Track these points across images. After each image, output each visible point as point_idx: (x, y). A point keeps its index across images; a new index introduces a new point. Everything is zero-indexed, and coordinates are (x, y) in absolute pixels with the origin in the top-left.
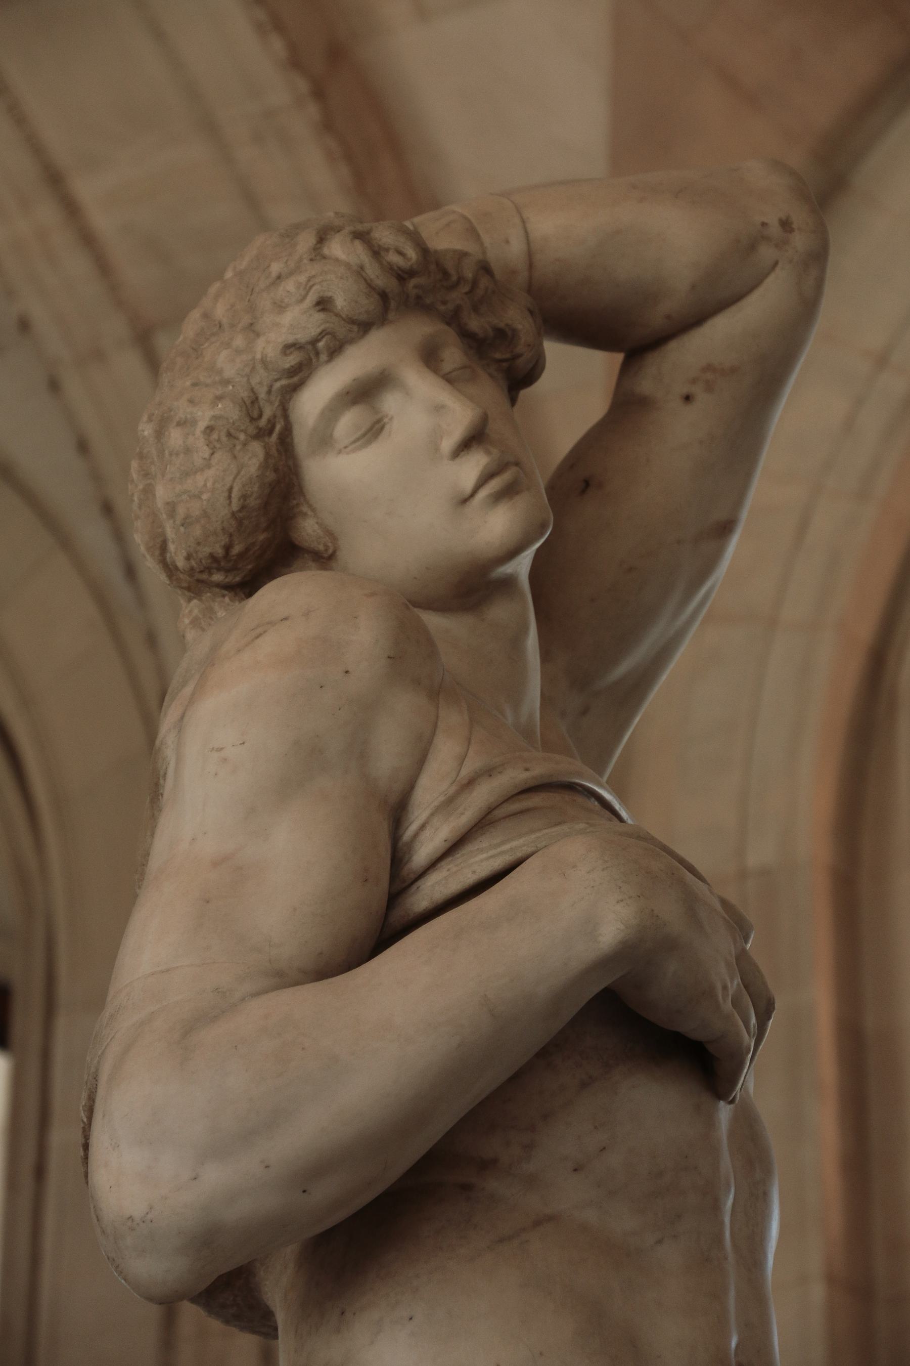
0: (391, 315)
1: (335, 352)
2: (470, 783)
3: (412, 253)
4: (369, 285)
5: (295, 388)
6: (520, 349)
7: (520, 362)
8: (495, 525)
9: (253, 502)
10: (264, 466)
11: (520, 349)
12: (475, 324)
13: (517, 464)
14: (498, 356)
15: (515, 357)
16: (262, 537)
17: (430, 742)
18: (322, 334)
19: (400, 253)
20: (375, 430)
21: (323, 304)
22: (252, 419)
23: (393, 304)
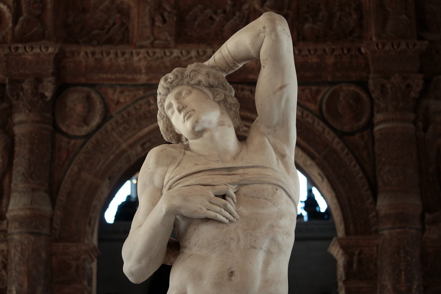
0: (171, 91)
1: (164, 101)
2: (168, 182)
3: (172, 78)
4: (164, 88)
5: (164, 109)
6: (203, 83)
7: (205, 84)
8: (189, 124)
9: (165, 131)
10: (164, 124)
11: (203, 83)
12: (193, 82)
13: (193, 110)
14: (202, 85)
15: (204, 84)
16: (171, 135)
17: (165, 175)
18: (161, 99)
19: (171, 78)
20: (173, 112)
21: (160, 94)
22: (161, 116)
23: (170, 89)
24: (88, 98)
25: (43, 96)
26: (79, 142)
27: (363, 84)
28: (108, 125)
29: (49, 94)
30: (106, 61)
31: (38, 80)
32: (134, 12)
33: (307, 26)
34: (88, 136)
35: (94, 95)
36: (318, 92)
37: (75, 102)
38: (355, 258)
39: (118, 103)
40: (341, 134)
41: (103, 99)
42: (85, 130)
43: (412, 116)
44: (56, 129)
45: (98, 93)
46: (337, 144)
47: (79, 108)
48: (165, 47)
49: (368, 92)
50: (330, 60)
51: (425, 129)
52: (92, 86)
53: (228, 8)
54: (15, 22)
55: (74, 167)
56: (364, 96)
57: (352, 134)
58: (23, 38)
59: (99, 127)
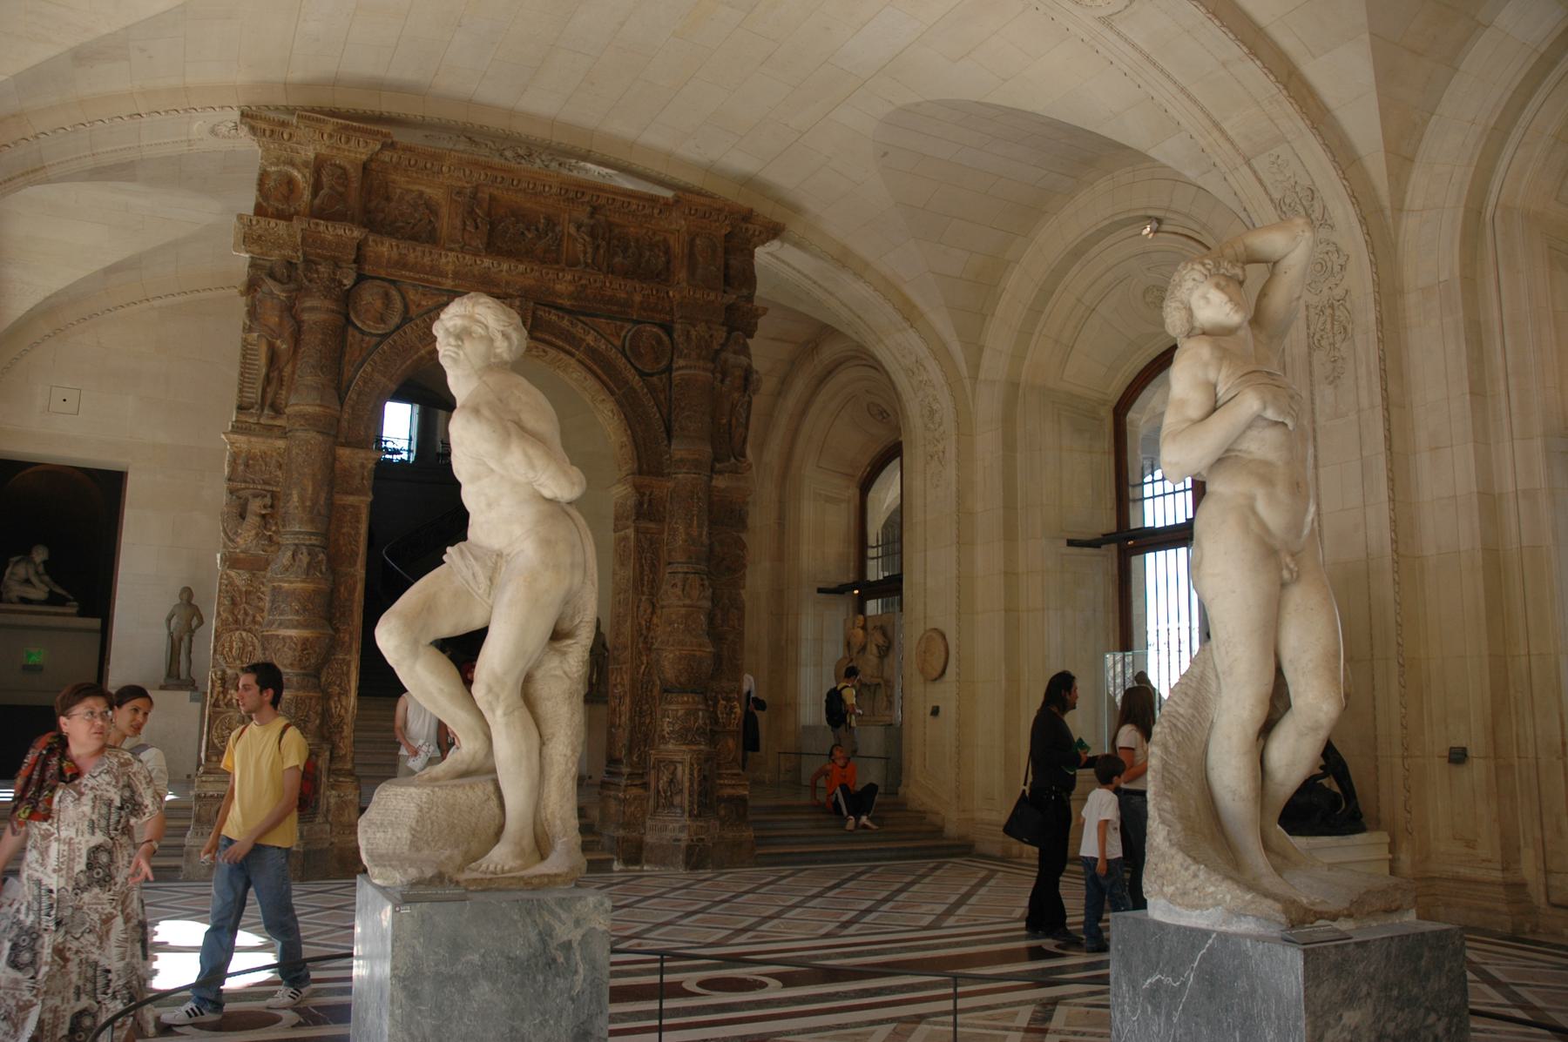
24: (387, 295)
25: (341, 284)
26: (375, 340)
27: (668, 328)
28: (407, 328)
29: (348, 282)
30: (411, 257)
31: (336, 263)
32: (444, 211)
33: (617, 260)
34: (385, 336)
35: (394, 293)
36: (622, 328)
37: (370, 297)
38: (646, 498)
39: (419, 306)
40: (642, 374)
41: (404, 298)
42: (382, 329)
43: (710, 366)
44: (348, 321)
45: (399, 291)
46: (635, 380)
47: (378, 304)
48: (476, 254)
49: (670, 336)
50: (638, 298)
51: (722, 381)
52: (393, 282)
53: (541, 226)
54: (315, 194)
55: (367, 367)
56: (665, 338)
57: (652, 375)
58: (318, 213)
59: (398, 327)
